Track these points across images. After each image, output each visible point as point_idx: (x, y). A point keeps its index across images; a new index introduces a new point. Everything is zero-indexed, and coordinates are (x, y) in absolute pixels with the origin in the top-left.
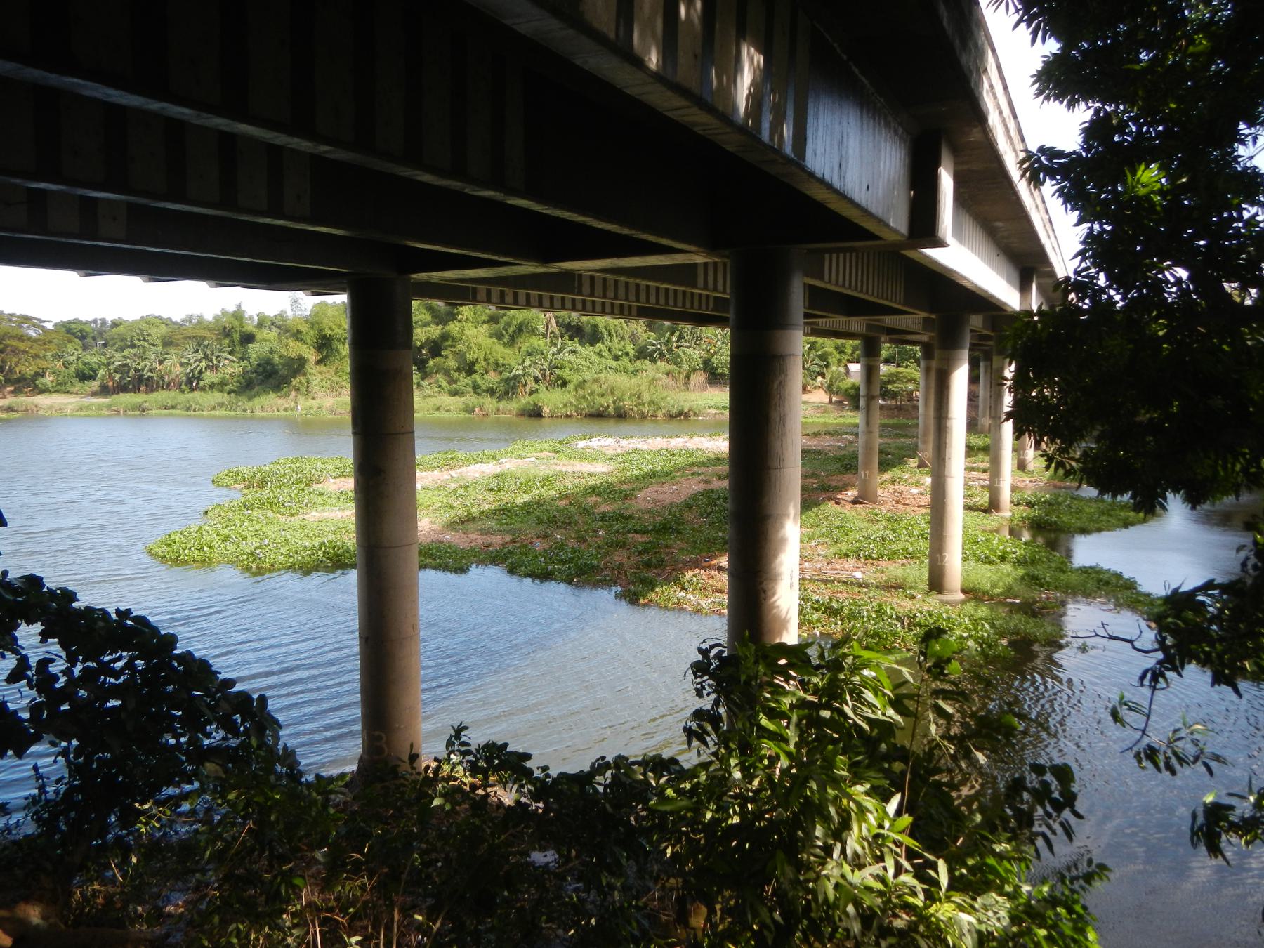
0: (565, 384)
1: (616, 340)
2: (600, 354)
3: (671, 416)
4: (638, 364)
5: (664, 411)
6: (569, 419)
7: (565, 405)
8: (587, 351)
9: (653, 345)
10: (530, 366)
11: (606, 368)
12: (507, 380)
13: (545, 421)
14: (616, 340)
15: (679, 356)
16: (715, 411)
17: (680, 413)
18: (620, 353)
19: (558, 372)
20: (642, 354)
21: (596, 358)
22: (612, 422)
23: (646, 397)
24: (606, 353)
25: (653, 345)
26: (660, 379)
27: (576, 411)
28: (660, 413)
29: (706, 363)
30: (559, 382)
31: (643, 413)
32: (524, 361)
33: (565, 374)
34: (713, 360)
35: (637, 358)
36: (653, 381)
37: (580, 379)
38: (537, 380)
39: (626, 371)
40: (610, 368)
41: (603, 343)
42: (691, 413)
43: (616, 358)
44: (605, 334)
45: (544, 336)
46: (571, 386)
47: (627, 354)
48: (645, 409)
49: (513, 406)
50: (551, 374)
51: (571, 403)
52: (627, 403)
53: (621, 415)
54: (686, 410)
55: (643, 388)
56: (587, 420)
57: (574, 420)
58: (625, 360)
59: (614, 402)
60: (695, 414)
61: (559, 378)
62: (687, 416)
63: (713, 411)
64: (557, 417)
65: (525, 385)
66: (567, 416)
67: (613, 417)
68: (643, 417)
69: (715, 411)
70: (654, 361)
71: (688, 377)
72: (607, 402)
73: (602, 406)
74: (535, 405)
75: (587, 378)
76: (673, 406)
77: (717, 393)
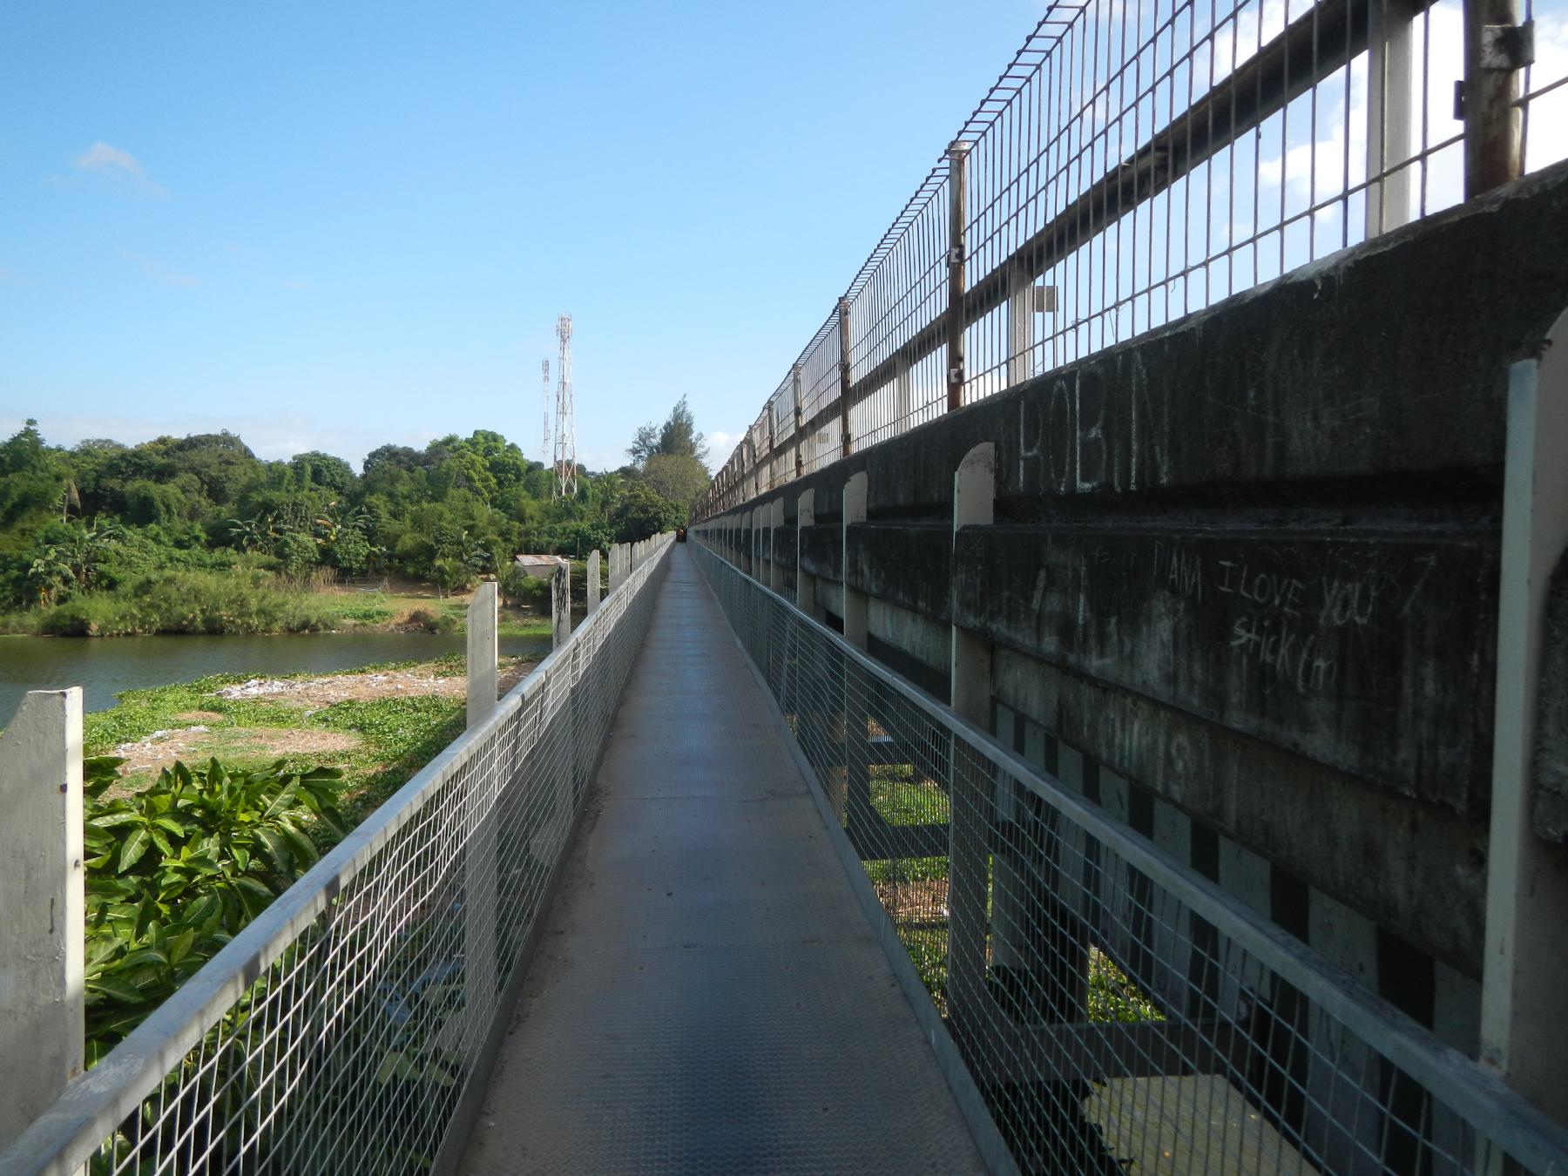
0: (112, 585)
1: (176, 517)
2: (156, 539)
3: (291, 630)
4: (217, 553)
5: (281, 624)
6: (130, 640)
7: (123, 618)
8: (135, 534)
9: (234, 525)
10: (57, 559)
11: (171, 559)
12: (17, 582)
13: (95, 643)
14: (176, 517)
15: (286, 544)
16: (353, 621)
17: (305, 625)
18: (185, 537)
19: (101, 567)
20: (219, 537)
21: (151, 544)
22: (200, 641)
23: (253, 604)
24: (165, 538)
25: (234, 525)
26: (264, 576)
27: (141, 627)
28: (277, 628)
29: (327, 557)
30: (104, 583)
31: (249, 626)
32: (47, 552)
33: (111, 569)
34: (337, 549)
35: (211, 546)
36: (256, 581)
37: (142, 578)
38: (66, 581)
39: (201, 565)
40: (178, 560)
41: (158, 523)
42: (320, 626)
43: (180, 544)
44: (162, 508)
45: (60, 511)
46: (127, 588)
47: (197, 539)
48: (255, 621)
49: (31, 619)
50: (88, 570)
51: (133, 616)
52: (225, 614)
53: (215, 630)
54: (313, 621)
55: (244, 591)
56: (159, 642)
57: (138, 640)
58: (197, 550)
59: (203, 611)
60: (326, 626)
61: (101, 575)
62: (314, 629)
63: (350, 622)
64: (111, 636)
65: (49, 587)
66: (127, 634)
67: (202, 633)
68: (250, 632)
69: (353, 621)
70: (240, 549)
71: (308, 575)
72: (193, 613)
73: (185, 618)
74: (73, 618)
75: (154, 576)
76: (294, 616)
77: (343, 594)
